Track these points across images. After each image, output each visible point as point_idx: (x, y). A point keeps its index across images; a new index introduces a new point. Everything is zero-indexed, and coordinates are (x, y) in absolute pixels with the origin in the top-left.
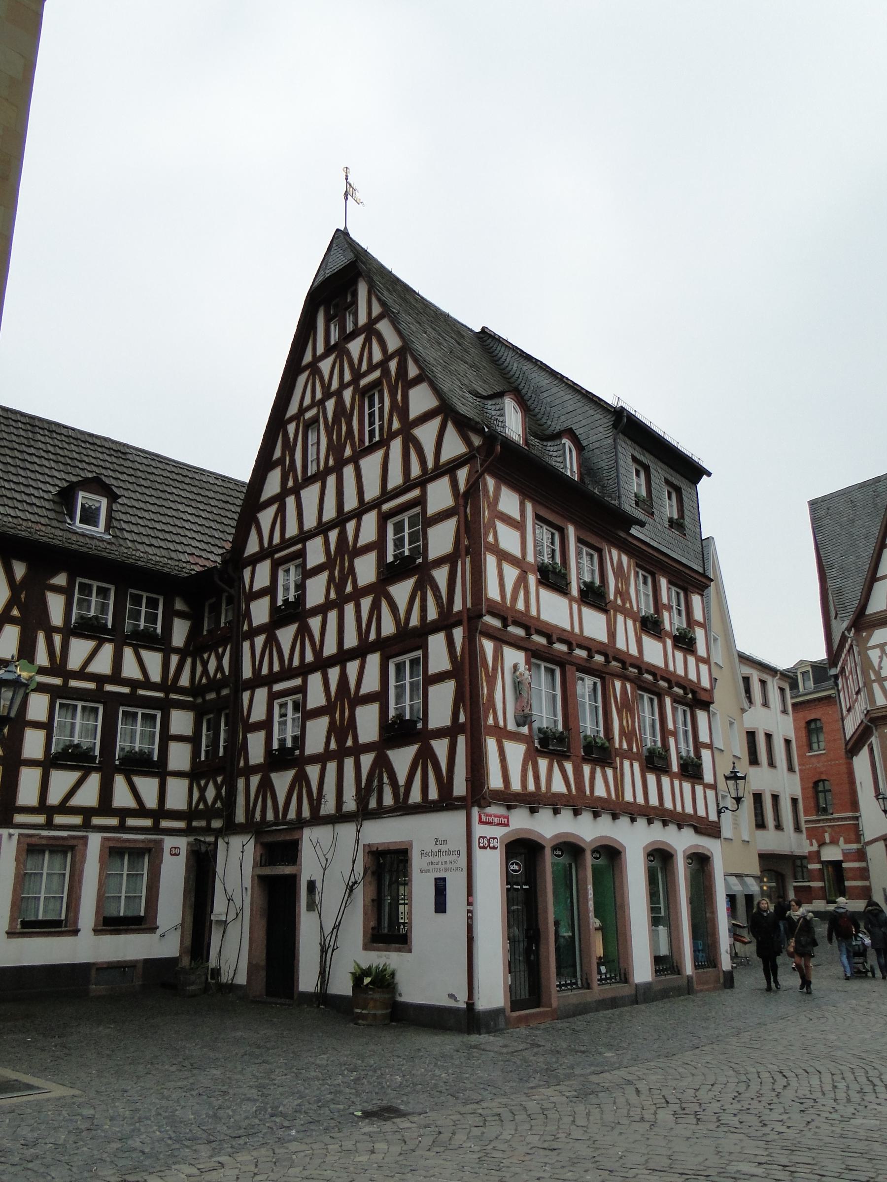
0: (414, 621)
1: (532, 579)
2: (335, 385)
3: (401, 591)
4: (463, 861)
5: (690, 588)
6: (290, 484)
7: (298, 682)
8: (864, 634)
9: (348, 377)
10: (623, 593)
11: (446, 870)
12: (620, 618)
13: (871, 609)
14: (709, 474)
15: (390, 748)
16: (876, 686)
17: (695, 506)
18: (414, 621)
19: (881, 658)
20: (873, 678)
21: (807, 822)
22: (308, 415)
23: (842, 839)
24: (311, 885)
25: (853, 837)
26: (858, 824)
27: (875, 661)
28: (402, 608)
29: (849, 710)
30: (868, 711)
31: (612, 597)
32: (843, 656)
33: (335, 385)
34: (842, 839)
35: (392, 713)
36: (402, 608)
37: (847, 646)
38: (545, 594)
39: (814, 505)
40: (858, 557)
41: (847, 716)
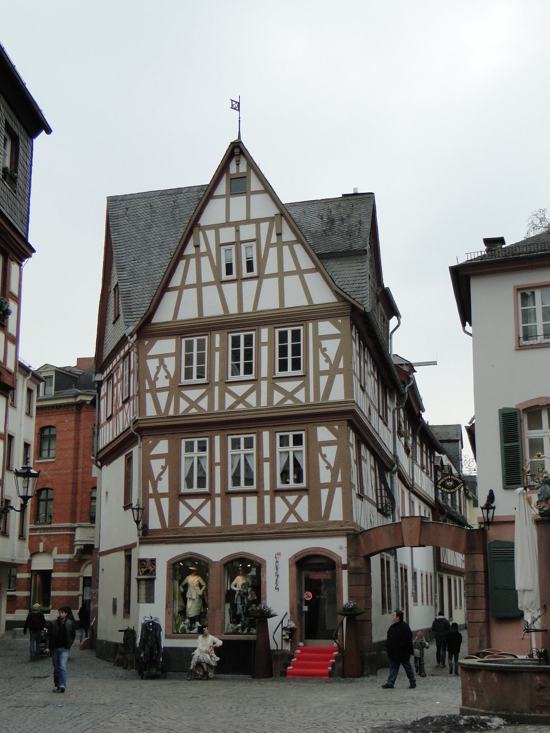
5: (11, 255)
8: (146, 342)
13: (158, 318)
14: (49, 131)
16: (149, 396)
17: (29, 162)
19: (158, 368)
20: (147, 387)
21: (31, 529)
23: (55, 550)
25: (67, 546)
26: (74, 535)
27: (153, 372)
29: (109, 419)
30: (137, 420)
32: (114, 362)
34: (55, 550)
37: (122, 353)
39: (113, 201)
40: (150, 264)
41: (105, 424)
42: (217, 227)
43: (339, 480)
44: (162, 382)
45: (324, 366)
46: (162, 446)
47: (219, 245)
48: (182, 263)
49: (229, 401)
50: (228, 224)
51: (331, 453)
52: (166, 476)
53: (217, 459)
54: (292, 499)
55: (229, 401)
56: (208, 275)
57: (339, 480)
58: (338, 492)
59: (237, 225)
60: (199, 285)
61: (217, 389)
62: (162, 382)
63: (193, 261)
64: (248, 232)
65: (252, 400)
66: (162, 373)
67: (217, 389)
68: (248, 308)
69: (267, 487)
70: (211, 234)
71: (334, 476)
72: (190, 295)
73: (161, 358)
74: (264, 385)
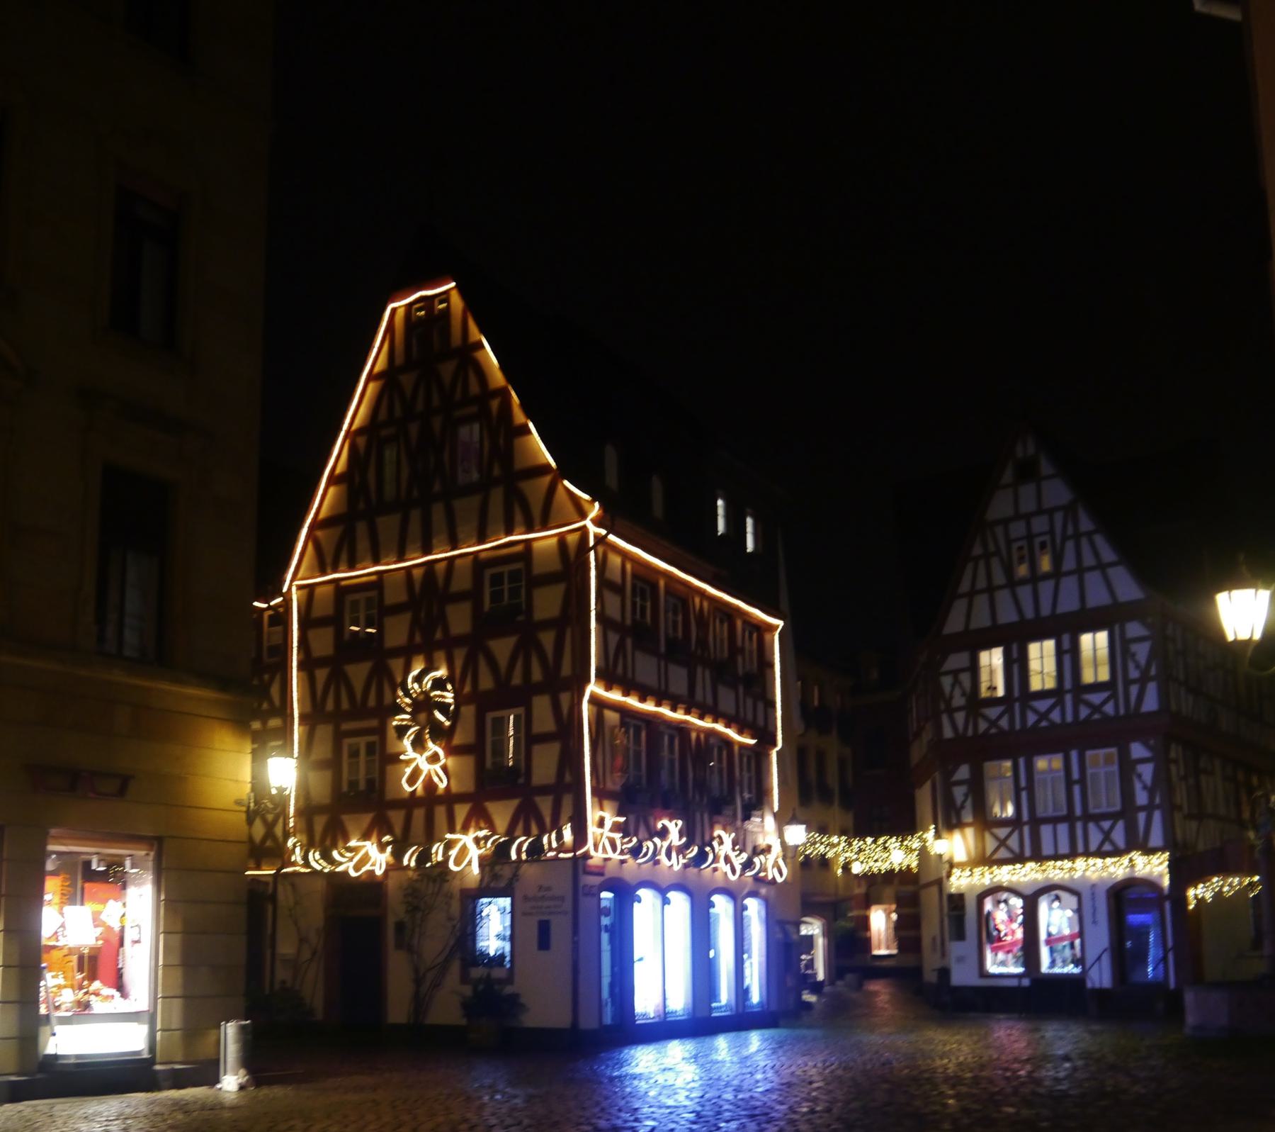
0: (517, 680)
1: (629, 642)
2: (420, 406)
3: (502, 648)
4: (568, 905)
6: (362, 506)
7: (374, 723)
9: (436, 401)
10: (702, 642)
11: (550, 913)
12: (699, 670)
15: (487, 800)
18: (517, 680)
19: (953, 686)
22: (384, 433)
24: (400, 927)
28: (503, 662)
31: (693, 648)
33: (420, 406)
35: (489, 763)
36: (503, 662)
38: (639, 656)
42: (1006, 522)
43: (1157, 800)
44: (958, 701)
45: (1134, 674)
46: (963, 772)
47: (1009, 542)
48: (970, 567)
49: (1031, 718)
50: (1017, 516)
51: (1147, 771)
52: (969, 804)
53: (1023, 783)
54: (1106, 825)
55: (1031, 718)
56: (999, 578)
57: (1157, 800)
58: (1157, 816)
59: (1028, 517)
60: (991, 590)
61: (1017, 706)
62: (958, 701)
63: (982, 565)
64: (1039, 524)
65: (1055, 716)
66: (957, 692)
67: (1017, 706)
68: (1046, 610)
69: (1078, 811)
70: (999, 530)
71: (1151, 798)
72: (981, 601)
73: (955, 673)
74: (1068, 698)
